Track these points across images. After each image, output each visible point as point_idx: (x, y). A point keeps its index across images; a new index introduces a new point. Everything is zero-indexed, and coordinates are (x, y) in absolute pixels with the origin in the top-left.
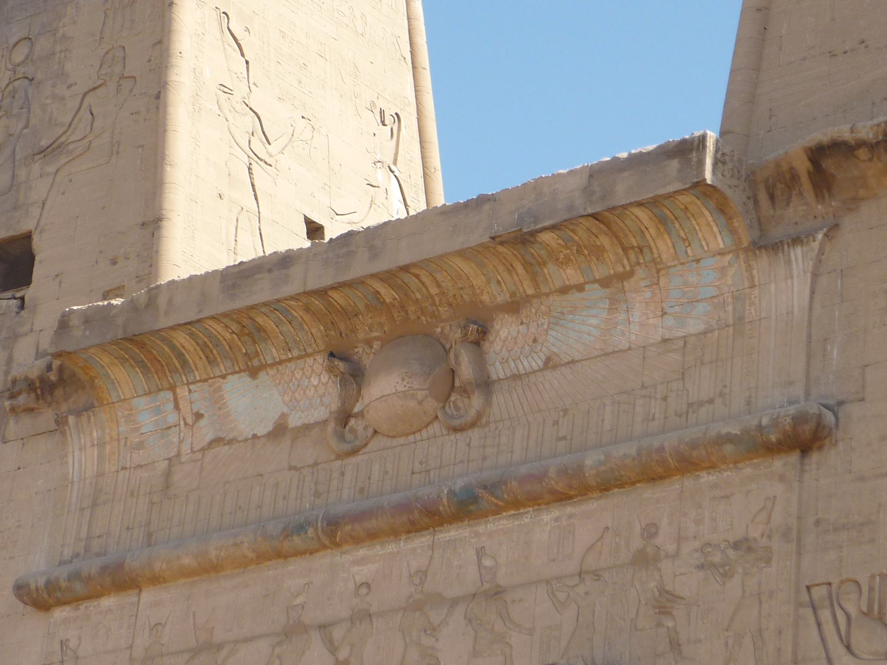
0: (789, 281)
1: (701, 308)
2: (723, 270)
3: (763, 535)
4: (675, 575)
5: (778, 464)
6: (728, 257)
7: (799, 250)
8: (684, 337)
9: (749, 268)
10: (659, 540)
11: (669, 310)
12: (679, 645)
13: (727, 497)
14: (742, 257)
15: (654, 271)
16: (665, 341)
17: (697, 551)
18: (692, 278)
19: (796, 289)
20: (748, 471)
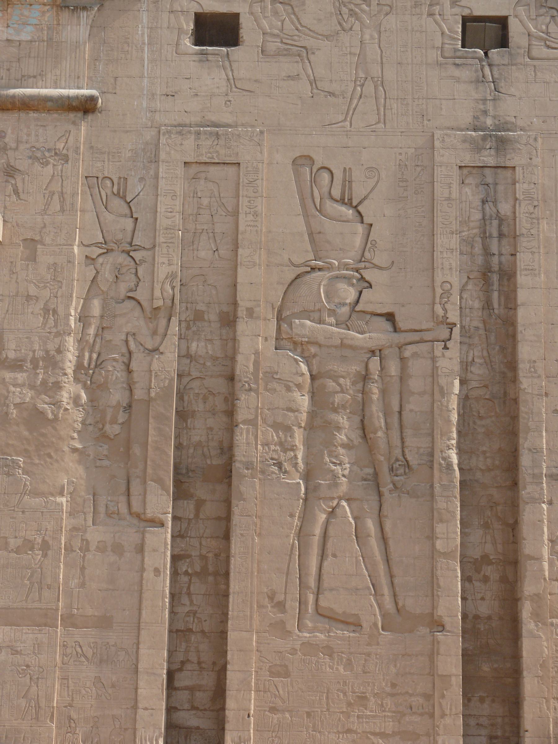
0: (78, 27)
1: (29, 28)
2: (43, 13)
3: (63, 148)
4: (16, 159)
5: (72, 115)
6: (48, 7)
7: (85, 14)
8: (19, 41)
9: (58, 15)
10: (6, 140)
11: (11, 25)
12: (18, 193)
13: (44, 126)
14: (55, 9)
15: (6, 4)
16: (8, 40)
17: (28, 149)
18: (26, 13)
19: (81, 31)
20: (55, 116)
